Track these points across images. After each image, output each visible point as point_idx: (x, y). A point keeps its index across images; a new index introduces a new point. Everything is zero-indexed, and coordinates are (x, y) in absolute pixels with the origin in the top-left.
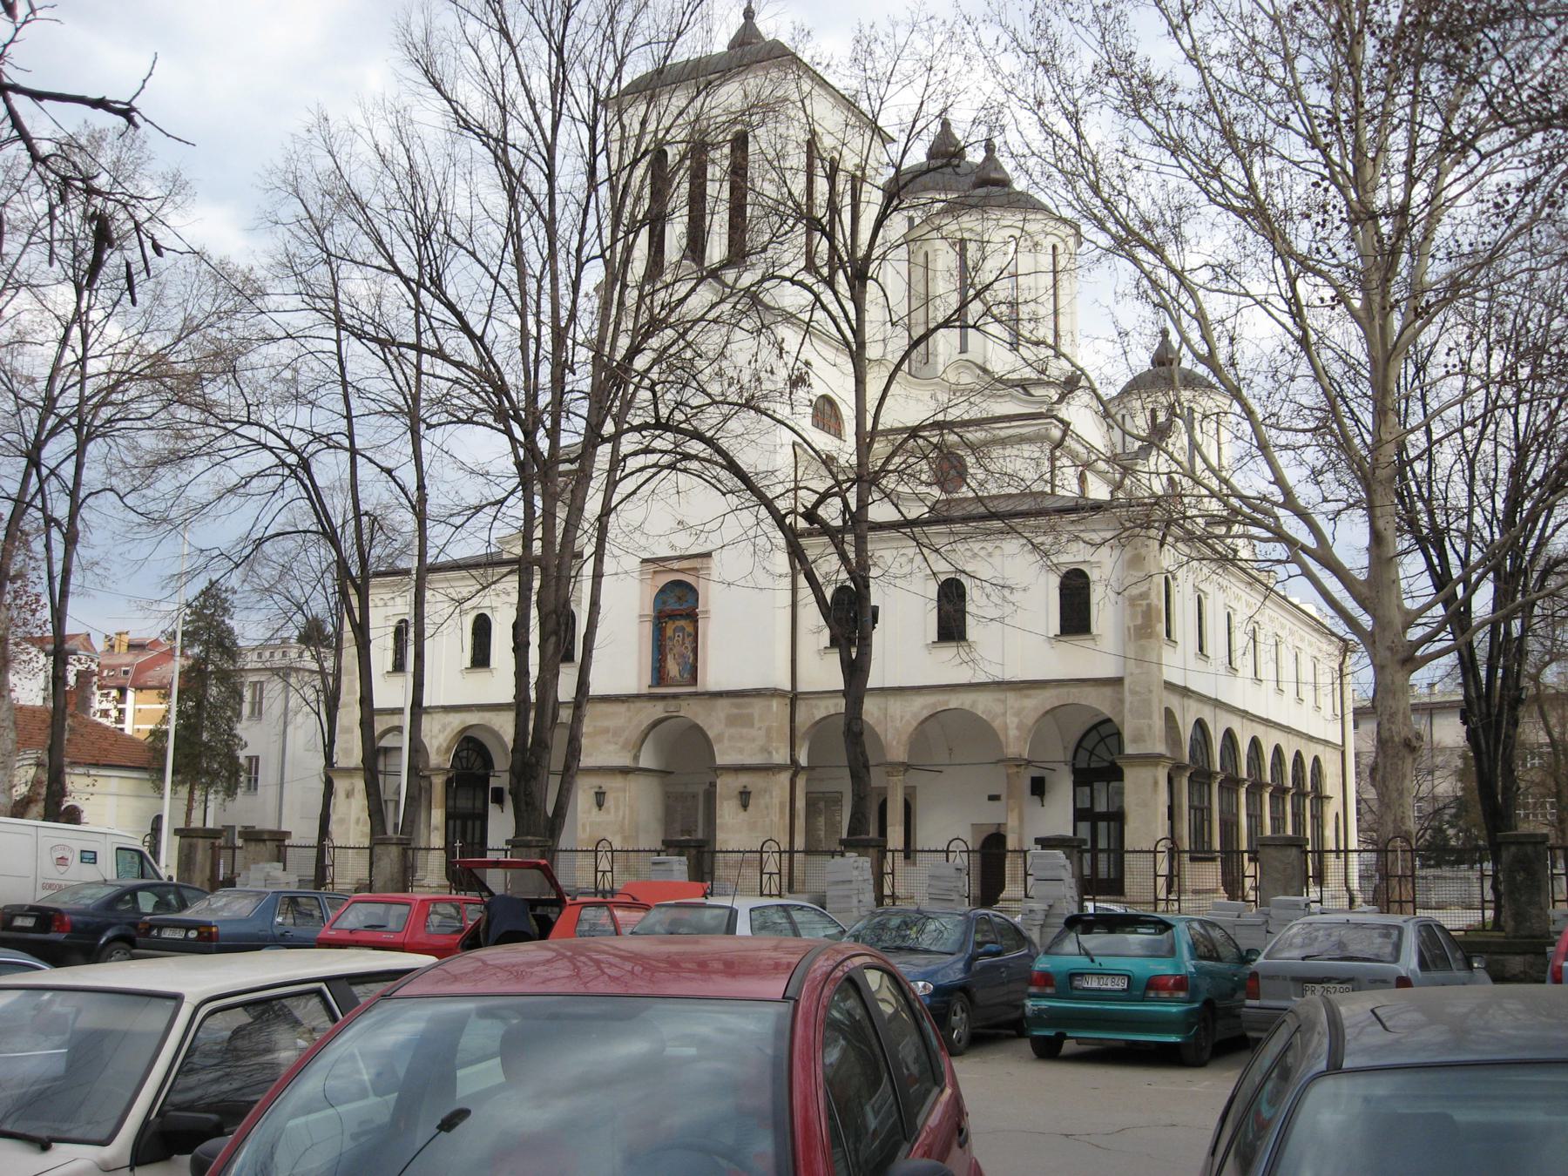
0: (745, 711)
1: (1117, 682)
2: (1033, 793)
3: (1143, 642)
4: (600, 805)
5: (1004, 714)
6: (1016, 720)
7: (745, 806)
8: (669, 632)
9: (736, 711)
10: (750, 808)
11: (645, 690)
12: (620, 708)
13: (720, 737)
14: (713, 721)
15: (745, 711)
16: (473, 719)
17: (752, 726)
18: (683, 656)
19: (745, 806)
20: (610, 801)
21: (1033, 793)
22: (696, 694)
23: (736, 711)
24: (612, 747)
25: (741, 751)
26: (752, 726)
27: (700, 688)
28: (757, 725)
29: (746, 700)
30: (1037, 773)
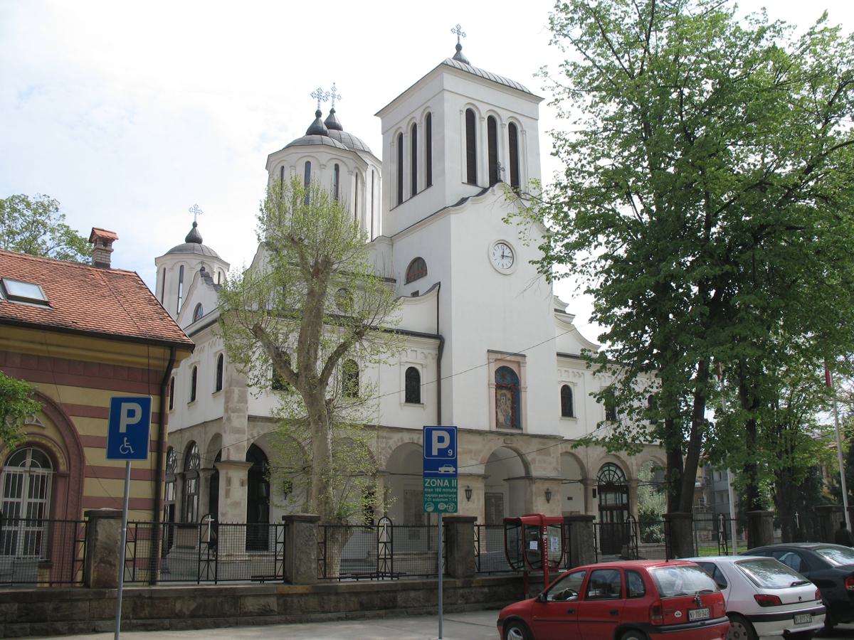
4: (469, 498)
7: (548, 501)
10: (550, 502)
11: (494, 428)
12: (479, 439)
13: (534, 460)
14: (530, 451)
18: (505, 411)
19: (548, 501)
20: (474, 497)
22: (522, 435)
24: (474, 462)
25: (545, 469)
26: (550, 455)
27: (524, 432)
28: (552, 455)
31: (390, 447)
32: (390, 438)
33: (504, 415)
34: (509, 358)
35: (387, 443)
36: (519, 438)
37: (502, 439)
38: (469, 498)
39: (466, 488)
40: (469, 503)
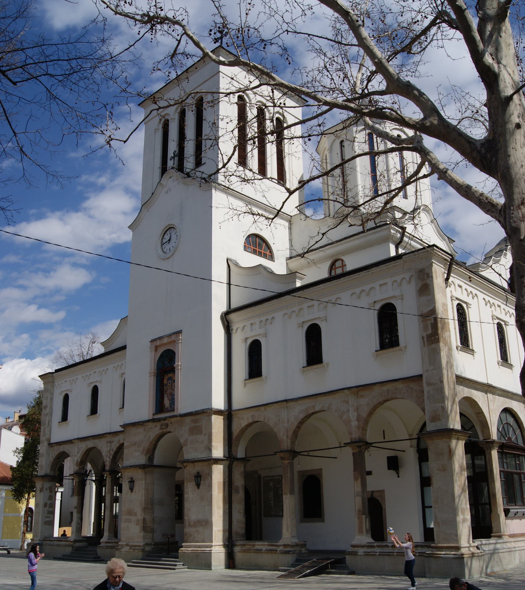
0: (198, 425)
1: (419, 378)
2: (389, 468)
3: (433, 346)
4: (132, 489)
5: (348, 411)
6: (356, 414)
8: (165, 382)
9: (193, 425)
10: (201, 487)
12: (141, 430)
13: (186, 441)
15: (198, 425)
16: (90, 444)
17: (202, 434)
20: (136, 488)
21: (389, 468)
22: (176, 416)
23: (193, 425)
24: (137, 454)
26: (202, 434)
27: (175, 413)
29: (198, 416)
30: (392, 454)
31: (112, 450)
32: (113, 442)
33: (169, 400)
34: (165, 340)
35: (111, 446)
36: (173, 420)
37: (158, 424)
38: (132, 489)
39: (129, 480)
40: (133, 493)
